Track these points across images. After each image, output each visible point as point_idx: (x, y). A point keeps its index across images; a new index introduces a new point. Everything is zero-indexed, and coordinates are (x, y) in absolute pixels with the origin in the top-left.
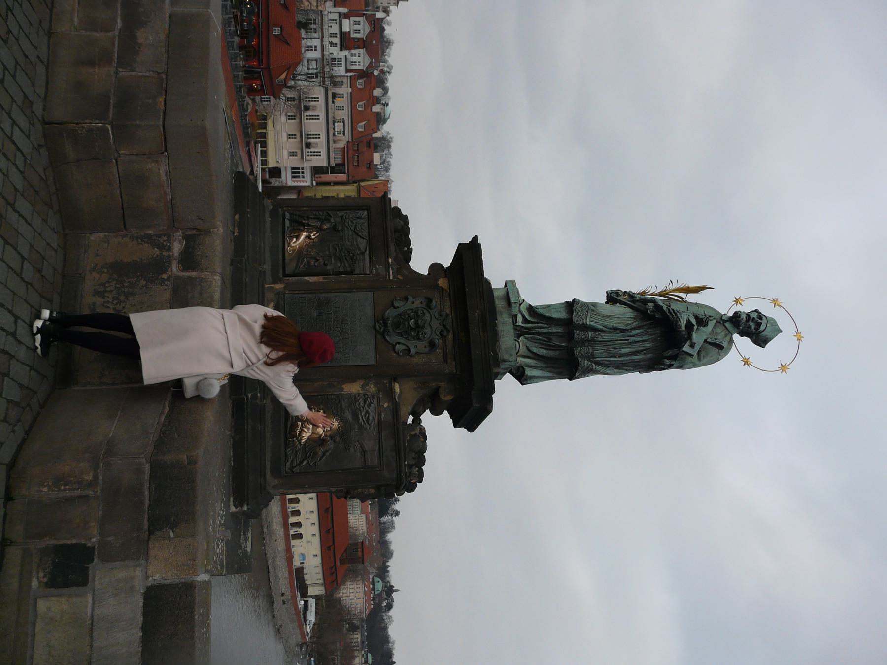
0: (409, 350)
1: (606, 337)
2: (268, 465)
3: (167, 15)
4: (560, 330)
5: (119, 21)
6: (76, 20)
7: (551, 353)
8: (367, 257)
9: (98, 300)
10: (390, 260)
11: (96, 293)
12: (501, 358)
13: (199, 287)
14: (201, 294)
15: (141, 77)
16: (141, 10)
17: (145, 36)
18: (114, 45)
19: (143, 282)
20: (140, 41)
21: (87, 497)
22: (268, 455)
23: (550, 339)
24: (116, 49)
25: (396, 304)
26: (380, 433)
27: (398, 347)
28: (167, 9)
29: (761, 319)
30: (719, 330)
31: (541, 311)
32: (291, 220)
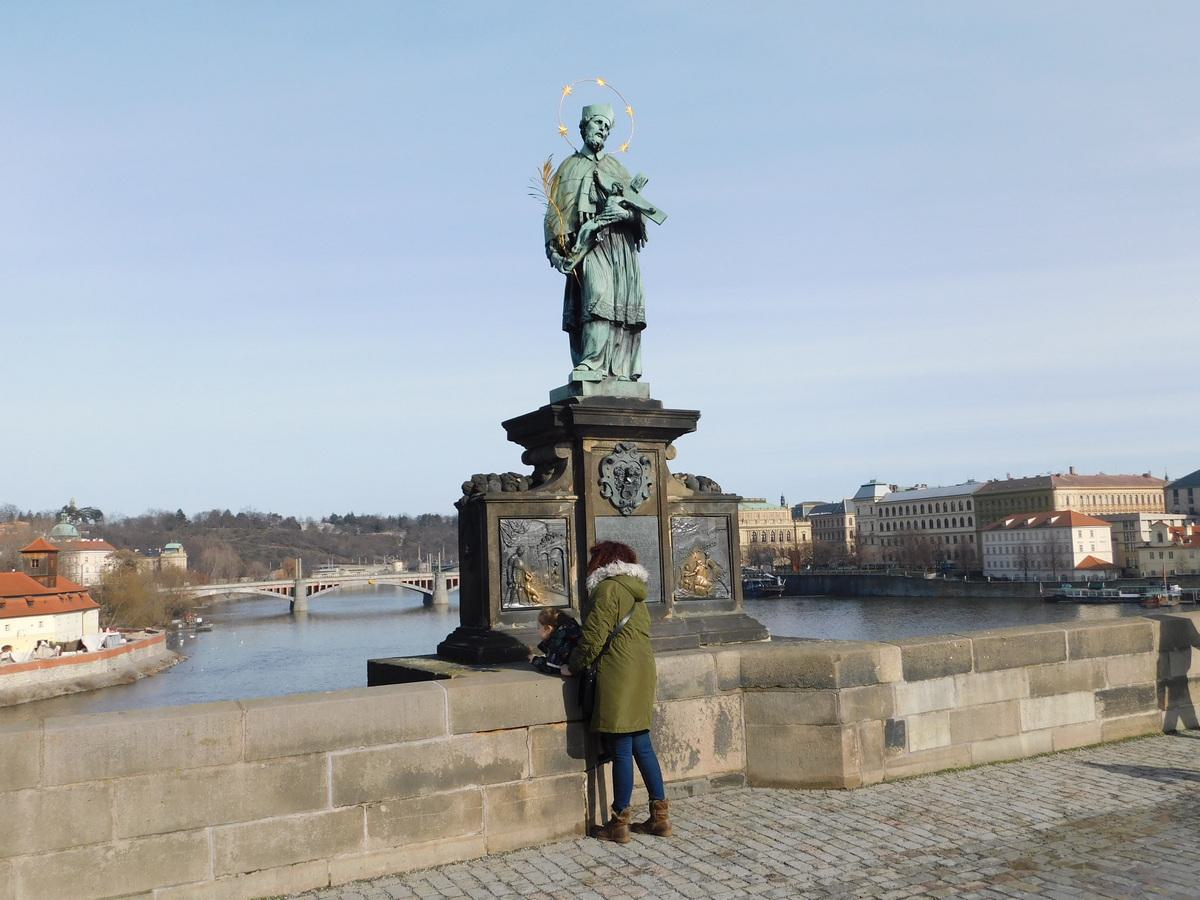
0: (649, 484)
1: (622, 289)
2: (727, 613)
3: (456, 737)
4: (613, 333)
5: (467, 788)
6: (470, 834)
7: (624, 346)
8: (549, 521)
9: (679, 767)
10: (558, 498)
11: (673, 769)
12: (645, 397)
13: (667, 677)
14: (672, 674)
15: (533, 752)
16: (451, 767)
17: (484, 759)
18: (499, 787)
19: (664, 729)
20: (490, 761)
21: (860, 731)
22: (719, 613)
23: (617, 345)
24: (503, 784)
25: (609, 495)
26: (703, 515)
27: (645, 495)
28: (450, 737)
29: (600, 122)
30: (607, 169)
31: (598, 350)
32: (511, 601)
